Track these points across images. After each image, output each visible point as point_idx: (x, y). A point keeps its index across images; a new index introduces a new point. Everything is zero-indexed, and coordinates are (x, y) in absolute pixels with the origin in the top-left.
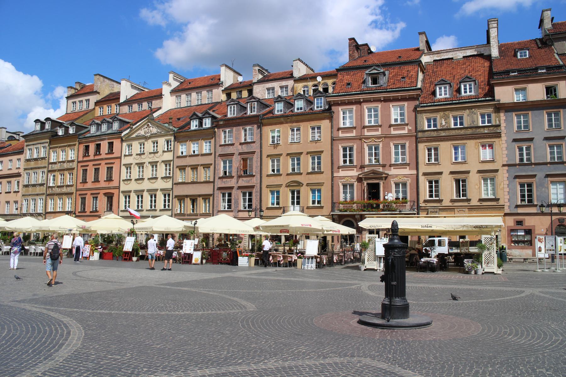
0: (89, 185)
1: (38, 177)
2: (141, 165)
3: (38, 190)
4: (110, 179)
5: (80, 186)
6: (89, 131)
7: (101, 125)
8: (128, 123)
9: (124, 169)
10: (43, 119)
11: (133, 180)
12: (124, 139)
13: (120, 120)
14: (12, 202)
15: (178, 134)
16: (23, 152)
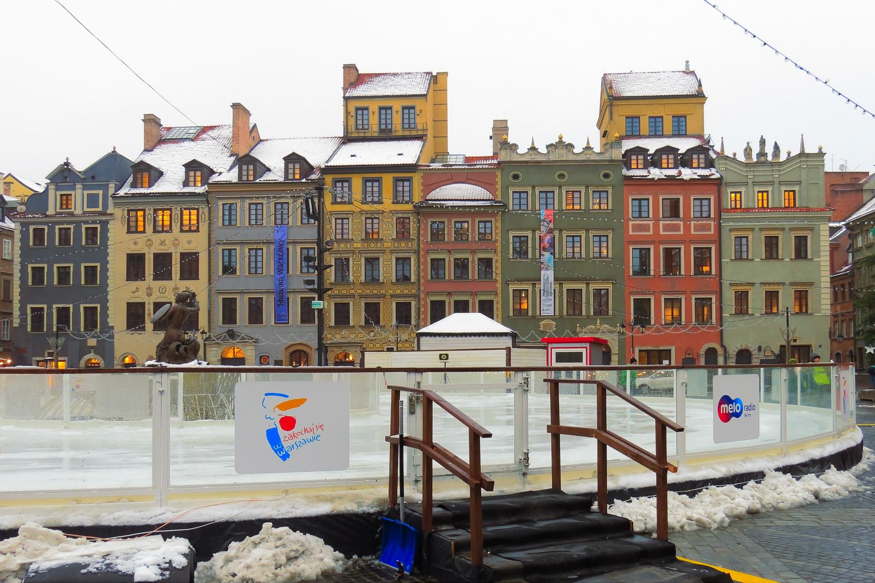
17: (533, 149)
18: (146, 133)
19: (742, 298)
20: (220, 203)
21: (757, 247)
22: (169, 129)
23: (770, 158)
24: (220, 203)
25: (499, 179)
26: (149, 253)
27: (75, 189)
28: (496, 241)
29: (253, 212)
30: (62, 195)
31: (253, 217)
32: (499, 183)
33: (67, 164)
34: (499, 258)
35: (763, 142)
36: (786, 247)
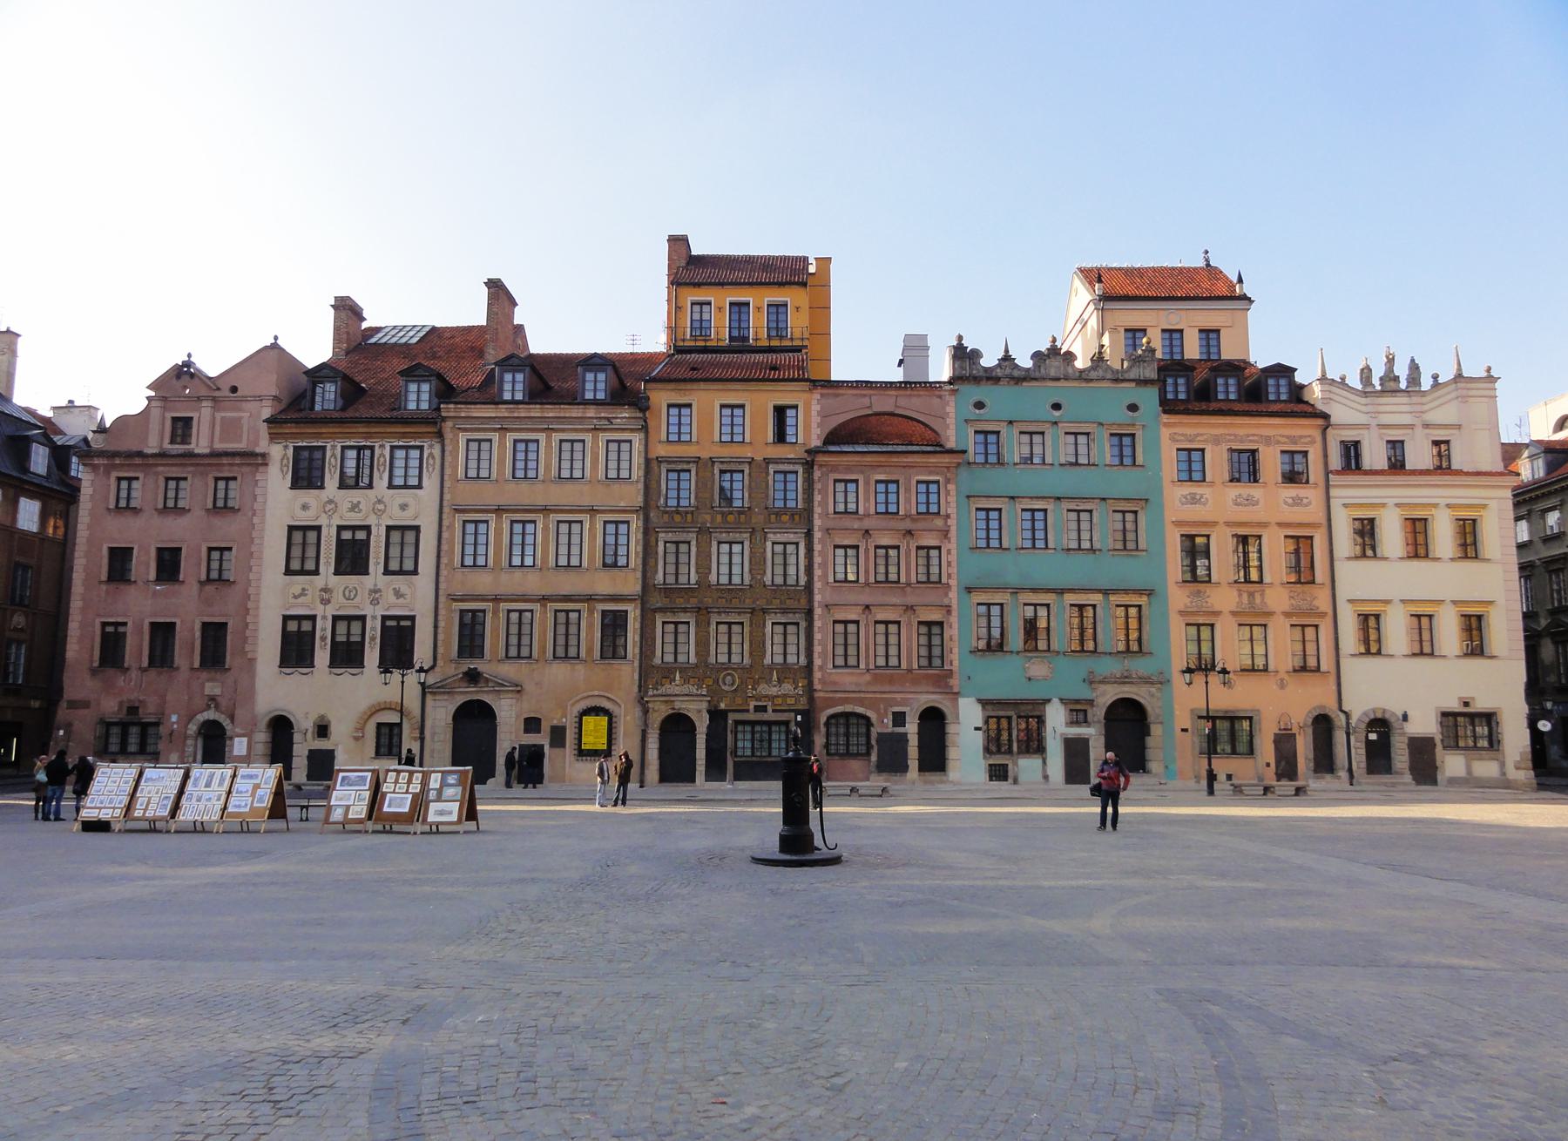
17: (1007, 358)
18: (337, 329)
20: (462, 438)
21: (1392, 536)
22: (377, 330)
23: (1403, 385)
24: (462, 438)
25: (951, 409)
26: (329, 526)
27: (198, 410)
28: (948, 516)
29: (521, 456)
30: (175, 420)
31: (520, 465)
32: (952, 415)
33: (187, 364)
34: (953, 546)
35: (1391, 361)
36: (1443, 536)
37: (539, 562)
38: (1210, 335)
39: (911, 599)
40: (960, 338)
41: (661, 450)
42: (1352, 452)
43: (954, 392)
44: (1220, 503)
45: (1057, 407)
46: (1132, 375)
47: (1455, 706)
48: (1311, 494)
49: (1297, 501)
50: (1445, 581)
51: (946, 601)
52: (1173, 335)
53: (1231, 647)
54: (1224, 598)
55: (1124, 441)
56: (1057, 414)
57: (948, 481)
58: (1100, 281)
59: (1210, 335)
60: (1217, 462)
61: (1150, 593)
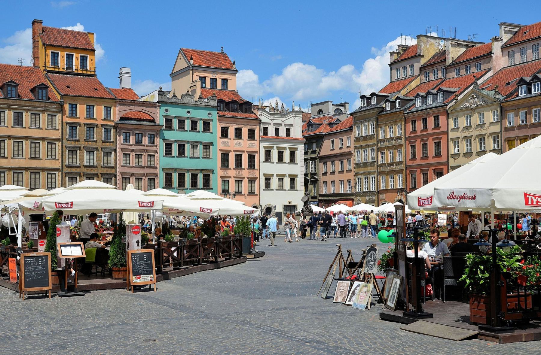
0: (418, 162)
1: (370, 155)
2: (468, 140)
3: (370, 169)
4: (438, 155)
5: (410, 163)
6: (415, 104)
7: (426, 97)
8: (454, 92)
9: (451, 144)
10: (368, 94)
11: (461, 155)
12: (449, 111)
13: (445, 91)
14: (345, 182)
15: (504, 104)
16: (352, 130)
17: (174, 96)
19: (268, 180)
28: (156, 146)
37: (24, 155)
38: (225, 82)
39: (146, 171)
40: (161, 88)
41: (66, 120)
42: (266, 129)
43: (159, 106)
44: (232, 144)
45: (189, 112)
46: (210, 104)
47: (287, 204)
48: (256, 143)
49: (252, 144)
50: (286, 169)
51: (156, 172)
52: (214, 81)
53: (232, 187)
54: (232, 173)
55: (207, 125)
56: (189, 114)
57: (157, 134)
58: (192, 59)
59: (225, 82)
60: (231, 132)
61: (212, 171)
